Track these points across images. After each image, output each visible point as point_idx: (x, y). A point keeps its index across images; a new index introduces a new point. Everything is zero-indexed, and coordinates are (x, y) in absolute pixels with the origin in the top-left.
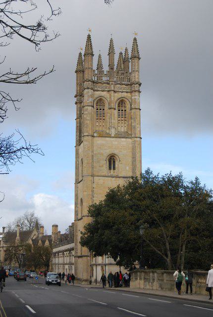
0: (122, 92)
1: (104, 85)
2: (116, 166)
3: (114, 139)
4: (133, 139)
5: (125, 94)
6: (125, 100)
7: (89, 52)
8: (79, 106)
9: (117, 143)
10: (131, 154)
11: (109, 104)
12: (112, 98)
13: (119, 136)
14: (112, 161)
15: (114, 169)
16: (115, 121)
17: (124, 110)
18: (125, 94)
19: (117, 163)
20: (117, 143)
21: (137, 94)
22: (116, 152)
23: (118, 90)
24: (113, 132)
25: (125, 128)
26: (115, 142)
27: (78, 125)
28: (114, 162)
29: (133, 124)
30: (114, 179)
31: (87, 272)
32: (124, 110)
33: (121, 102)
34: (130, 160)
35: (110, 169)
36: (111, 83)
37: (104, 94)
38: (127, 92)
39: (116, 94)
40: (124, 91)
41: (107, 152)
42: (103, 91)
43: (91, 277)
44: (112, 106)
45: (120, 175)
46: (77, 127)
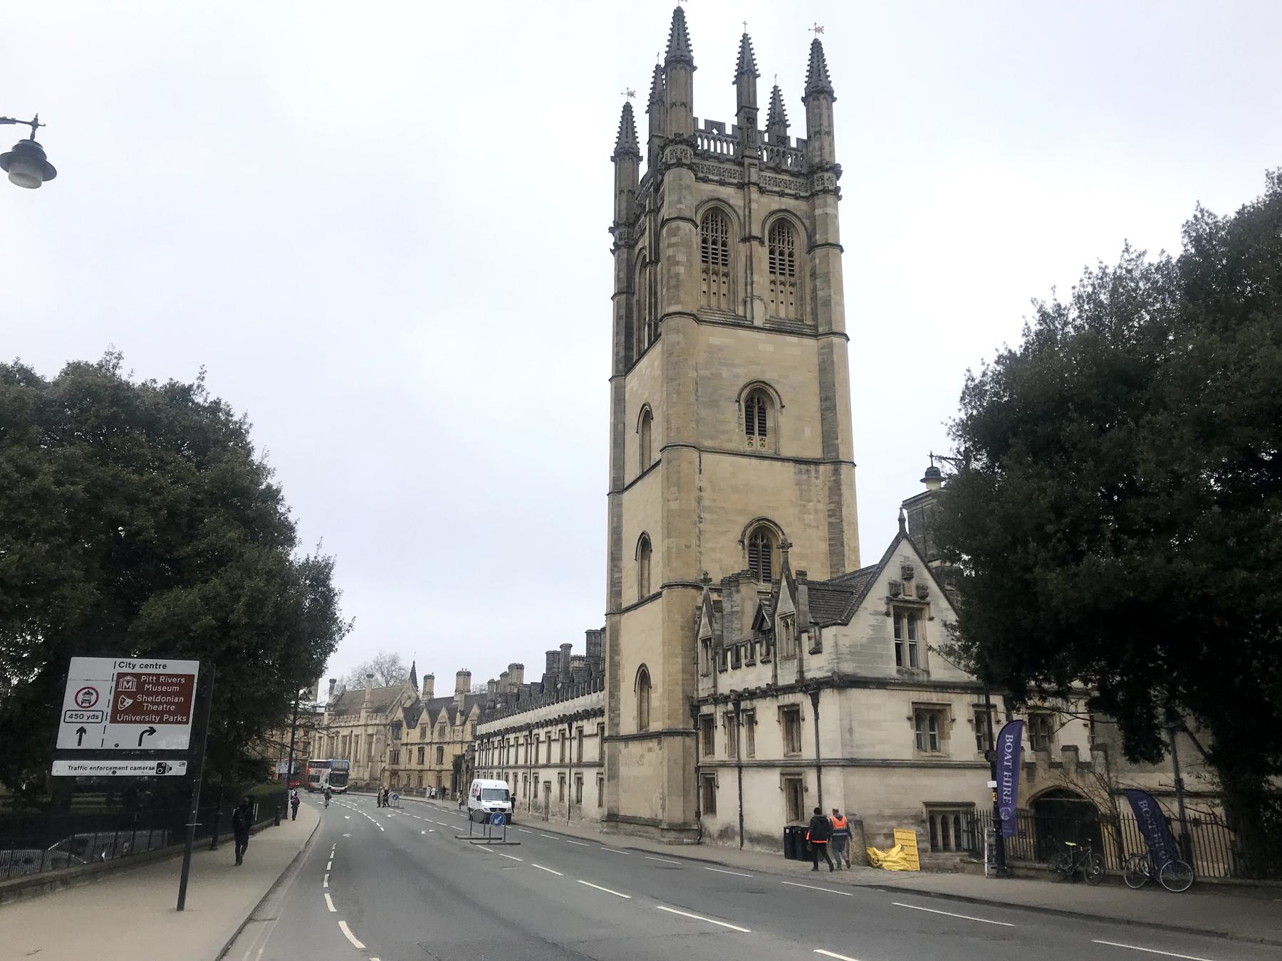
0: (782, 194)
1: (727, 166)
2: (770, 423)
3: (762, 335)
4: (823, 340)
5: (789, 203)
6: (794, 220)
7: (678, 62)
8: (625, 256)
9: (770, 348)
10: (815, 388)
11: (742, 226)
12: (754, 206)
13: (778, 328)
14: (757, 403)
15: (763, 432)
16: (762, 278)
17: (787, 251)
18: (789, 203)
19: (770, 413)
20: (770, 348)
21: (830, 199)
22: (768, 376)
23: (768, 188)
24: (760, 315)
25: (791, 309)
26: (767, 344)
27: (623, 312)
28: (762, 411)
29: (820, 294)
30: (767, 462)
31: (685, 794)
32: (787, 251)
33: (781, 226)
34: (813, 403)
35: (750, 431)
36: (747, 161)
37: (728, 193)
38: (796, 197)
39: (764, 199)
40: (787, 191)
41: (746, 374)
42: (722, 183)
43: (698, 814)
44: (756, 231)
45: (785, 453)
46: (618, 318)
